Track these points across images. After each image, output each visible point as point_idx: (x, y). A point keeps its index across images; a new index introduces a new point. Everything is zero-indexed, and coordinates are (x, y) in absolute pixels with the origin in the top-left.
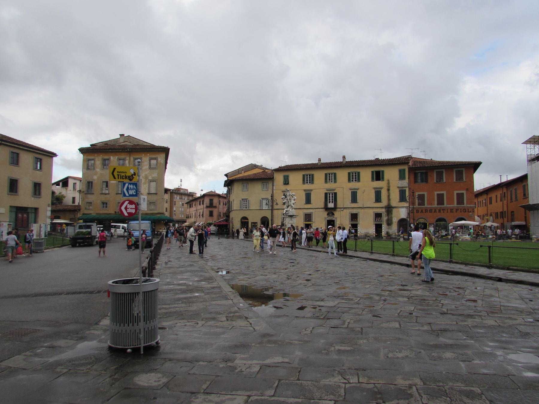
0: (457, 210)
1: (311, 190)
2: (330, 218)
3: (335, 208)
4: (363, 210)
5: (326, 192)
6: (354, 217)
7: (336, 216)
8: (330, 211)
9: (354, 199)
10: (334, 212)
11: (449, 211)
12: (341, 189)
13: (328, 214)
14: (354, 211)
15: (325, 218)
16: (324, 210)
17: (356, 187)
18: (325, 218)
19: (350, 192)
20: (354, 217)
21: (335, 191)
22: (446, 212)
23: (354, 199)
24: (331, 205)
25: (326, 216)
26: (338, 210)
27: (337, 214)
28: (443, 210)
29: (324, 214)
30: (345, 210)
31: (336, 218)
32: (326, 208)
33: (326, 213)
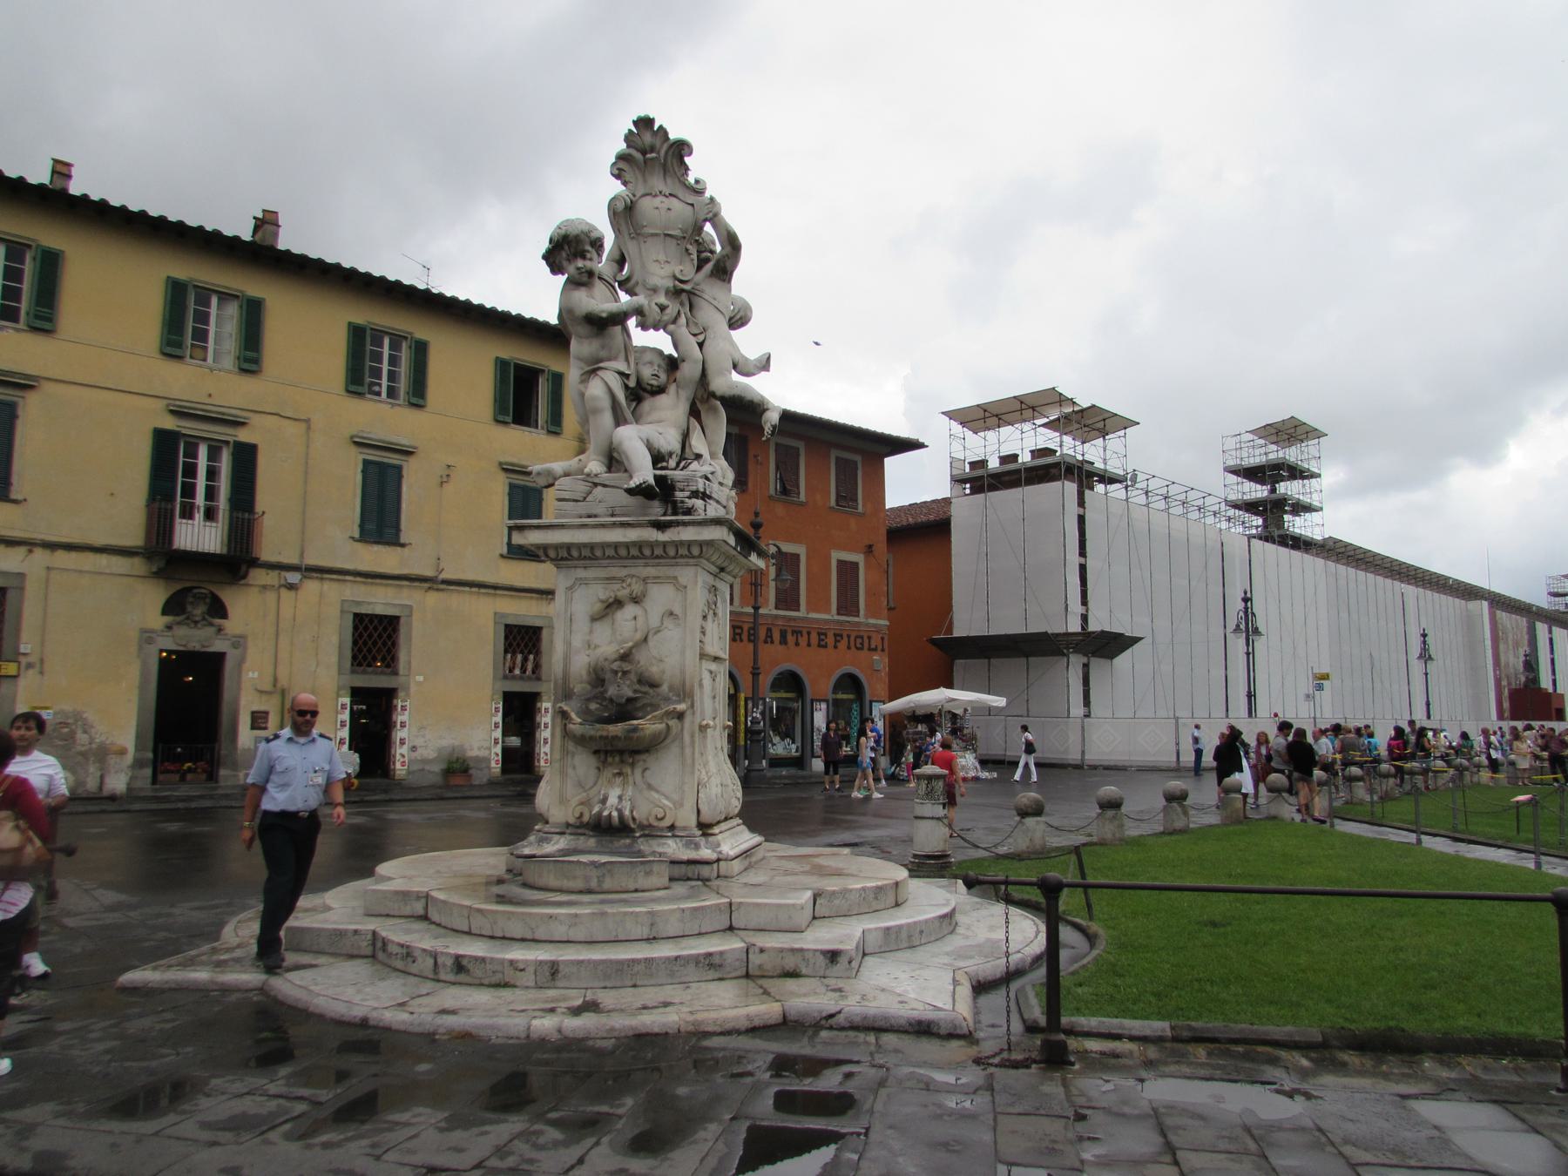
0: (838, 637)
1: (25, 384)
2: (195, 638)
3: (237, 562)
4: (432, 599)
5: (170, 423)
6: (375, 639)
7: (233, 625)
8: (196, 584)
9: (380, 516)
10: (230, 597)
11: (814, 638)
12: (292, 429)
13: (173, 607)
14: (380, 601)
15: (147, 637)
16: (137, 565)
17: (404, 441)
18: (147, 637)
19: (357, 458)
20: (375, 639)
21: (244, 436)
22: (803, 641)
23: (380, 516)
24: (200, 535)
25: (157, 621)
26: (258, 576)
27: (247, 608)
28: (797, 633)
29: (146, 603)
30: (312, 587)
31: (239, 642)
32: (162, 556)
33: (153, 596)
